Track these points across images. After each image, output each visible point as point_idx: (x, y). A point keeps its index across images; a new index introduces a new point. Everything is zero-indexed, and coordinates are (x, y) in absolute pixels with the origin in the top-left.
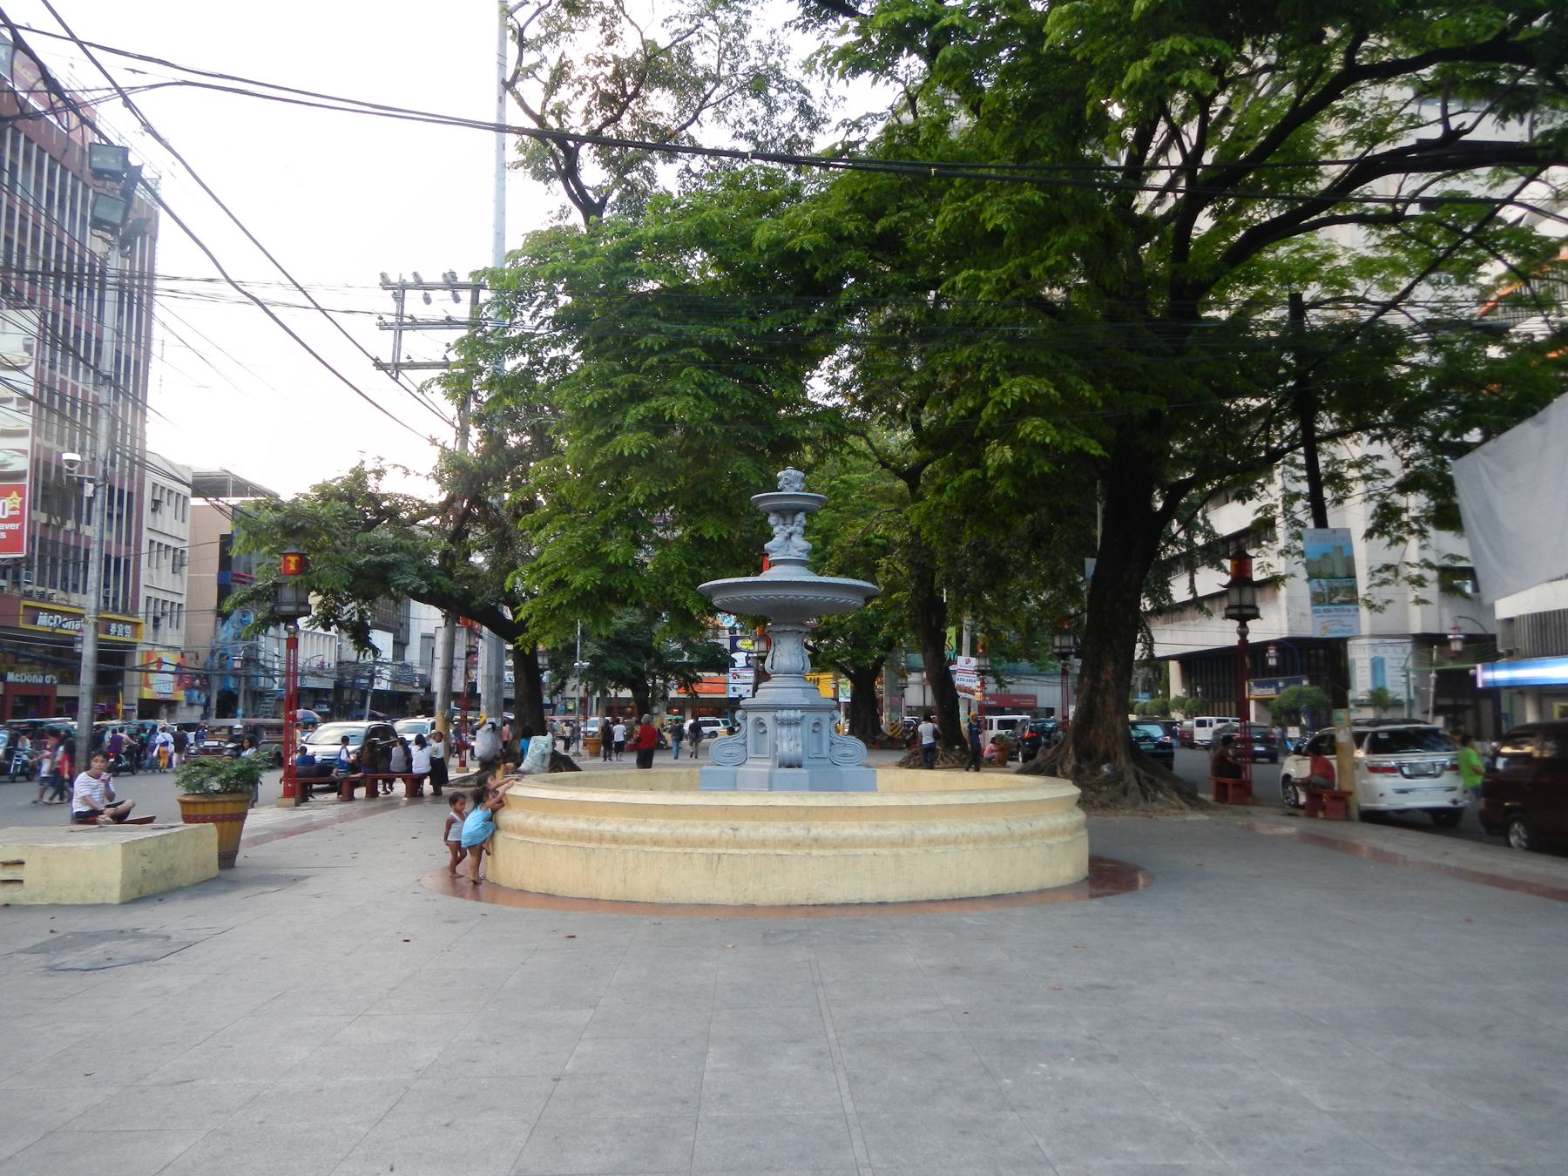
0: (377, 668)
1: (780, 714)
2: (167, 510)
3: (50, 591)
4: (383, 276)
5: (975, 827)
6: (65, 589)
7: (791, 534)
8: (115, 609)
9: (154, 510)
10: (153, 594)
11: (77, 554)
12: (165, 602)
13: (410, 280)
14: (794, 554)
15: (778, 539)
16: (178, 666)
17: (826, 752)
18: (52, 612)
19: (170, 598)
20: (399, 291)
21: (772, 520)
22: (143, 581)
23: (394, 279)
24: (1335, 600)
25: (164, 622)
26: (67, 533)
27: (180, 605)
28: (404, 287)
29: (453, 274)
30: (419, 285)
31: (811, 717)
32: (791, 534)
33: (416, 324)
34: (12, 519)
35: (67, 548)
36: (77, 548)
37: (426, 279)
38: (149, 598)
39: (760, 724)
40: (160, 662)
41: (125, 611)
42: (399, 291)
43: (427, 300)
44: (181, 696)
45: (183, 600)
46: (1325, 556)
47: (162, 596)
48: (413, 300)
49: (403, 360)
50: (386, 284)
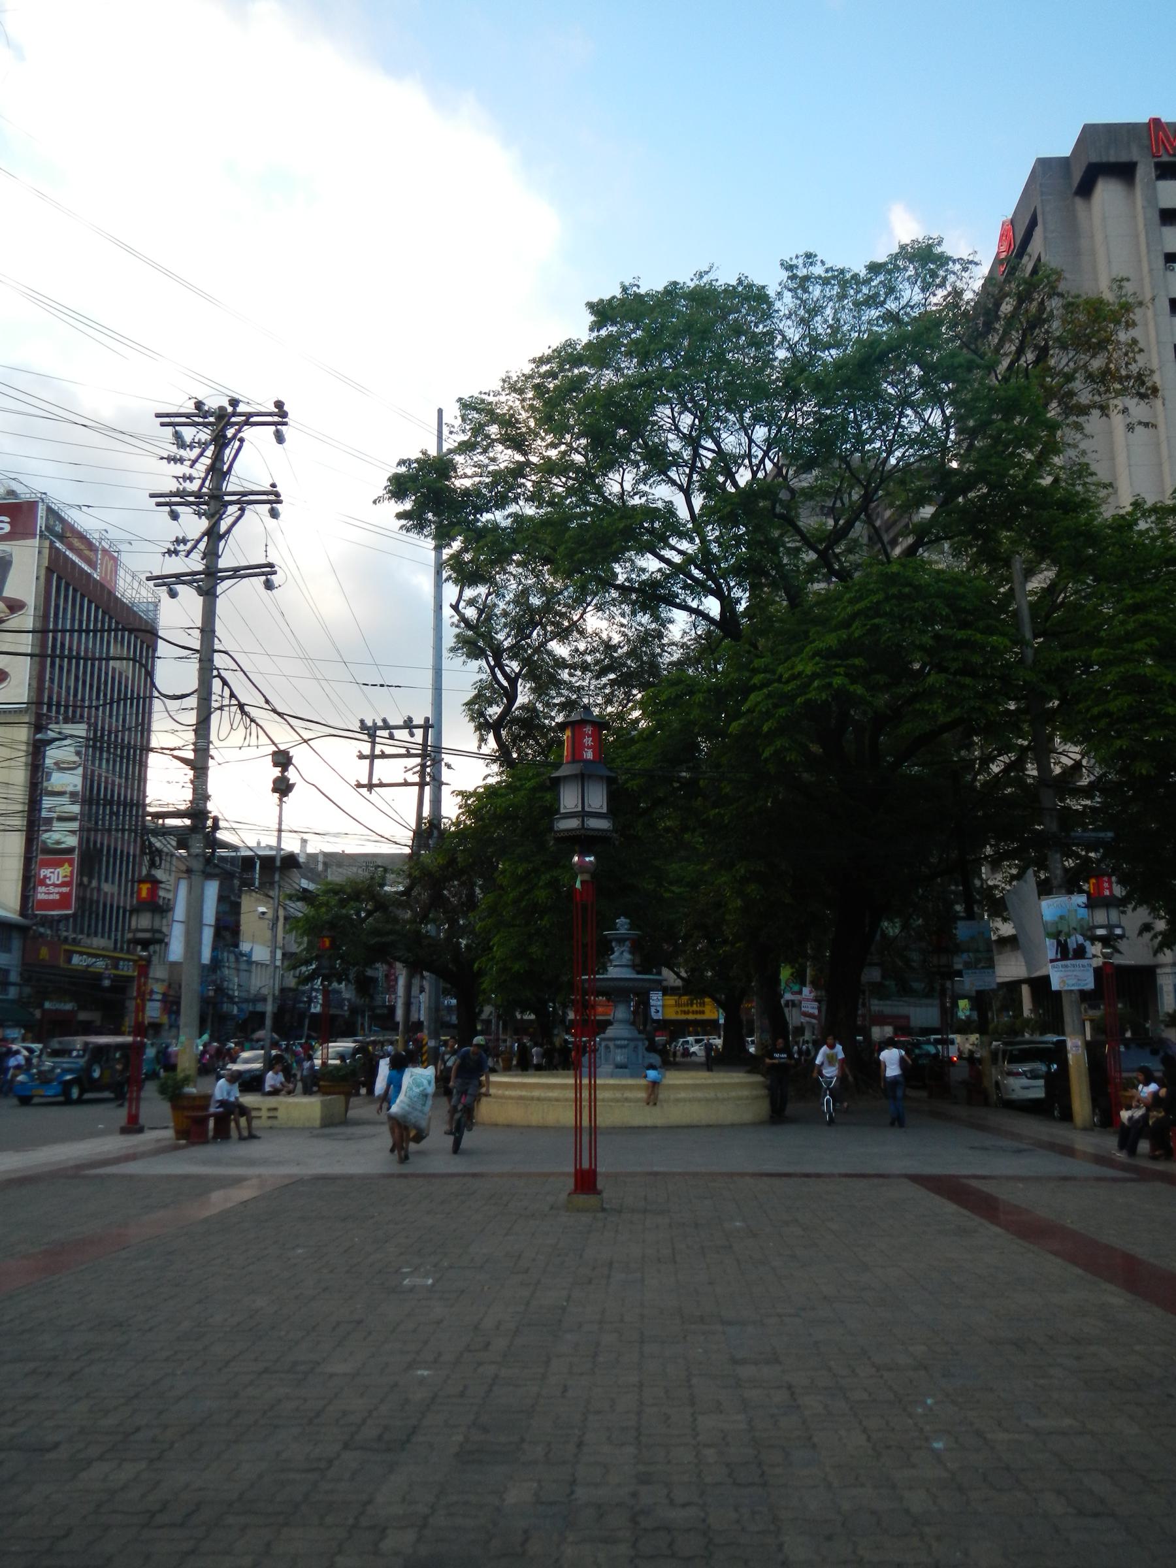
0: (314, 994)
1: (619, 1042)
3: (80, 937)
4: (362, 721)
5: (699, 1094)
7: (623, 952)
8: (122, 950)
11: (98, 907)
13: (380, 723)
14: (624, 962)
15: (616, 954)
17: (640, 1061)
18: (81, 953)
20: (370, 732)
21: (614, 944)
23: (369, 723)
24: (979, 966)
26: (92, 890)
28: (376, 728)
29: (410, 719)
30: (386, 726)
31: (632, 1044)
32: (623, 952)
33: (383, 756)
34: (63, 884)
36: (98, 902)
37: (392, 723)
39: (607, 1047)
46: (1062, 918)
49: (375, 781)
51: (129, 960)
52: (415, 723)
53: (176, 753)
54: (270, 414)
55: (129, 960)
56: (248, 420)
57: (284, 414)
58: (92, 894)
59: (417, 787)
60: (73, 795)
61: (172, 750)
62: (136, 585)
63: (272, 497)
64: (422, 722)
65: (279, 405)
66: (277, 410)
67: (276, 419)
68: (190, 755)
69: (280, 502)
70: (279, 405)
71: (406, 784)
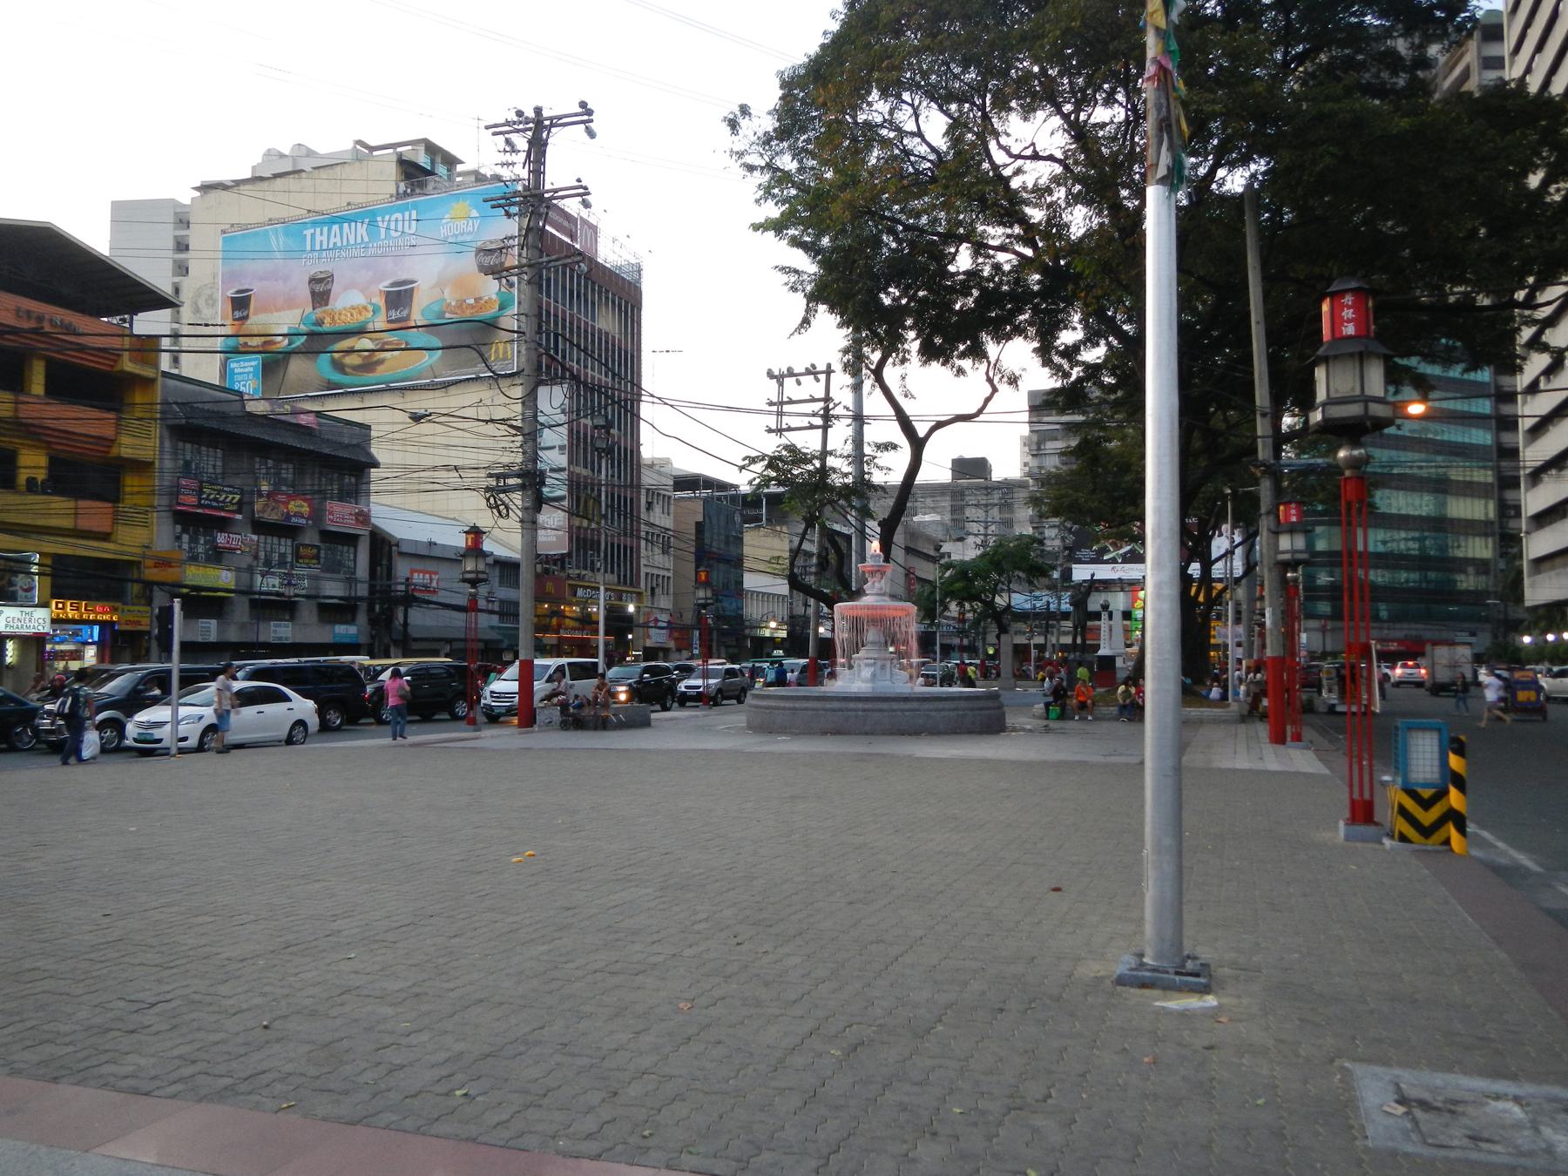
2: (657, 509)
3: (584, 572)
6: (592, 570)
8: (625, 583)
9: (648, 509)
10: (649, 570)
12: (658, 576)
16: (669, 622)
18: (585, 588)
19: (662, 573)
20: (780, 379)
22: (643, 561)
23: (776, 373)
25: (658, 591)
26: (593, 530)
27: (669, 578)
29: (813, 366)
30: (791, 373)
35: (592, 540)
38: (647, 574)
40: (657, 620)
41: (632, 585)
42: (780, 379)
43: (799, 383)
44: (672, 644)
45: (671, 574)
47: (656, 572)
48: (789, 382)
50: (770, 375)
51: (631, 592)
52: (818, 369)
53: (508, 422)
54: (576, 115)
55: (631, 592)
56: (556, 122)
57: (590, 112)
58: (592, 535)
59: (820, 430)
60: (562, 448)
61: (508, 419)
62: (617, 248)
63: (581, 191)
64: (824, 368)
65: (583, 105)
66: (580, 110)
67: (586, 118)
68: (519, 423)
69: (588, 194)
70: (583, 105)
71: (812, 427)
